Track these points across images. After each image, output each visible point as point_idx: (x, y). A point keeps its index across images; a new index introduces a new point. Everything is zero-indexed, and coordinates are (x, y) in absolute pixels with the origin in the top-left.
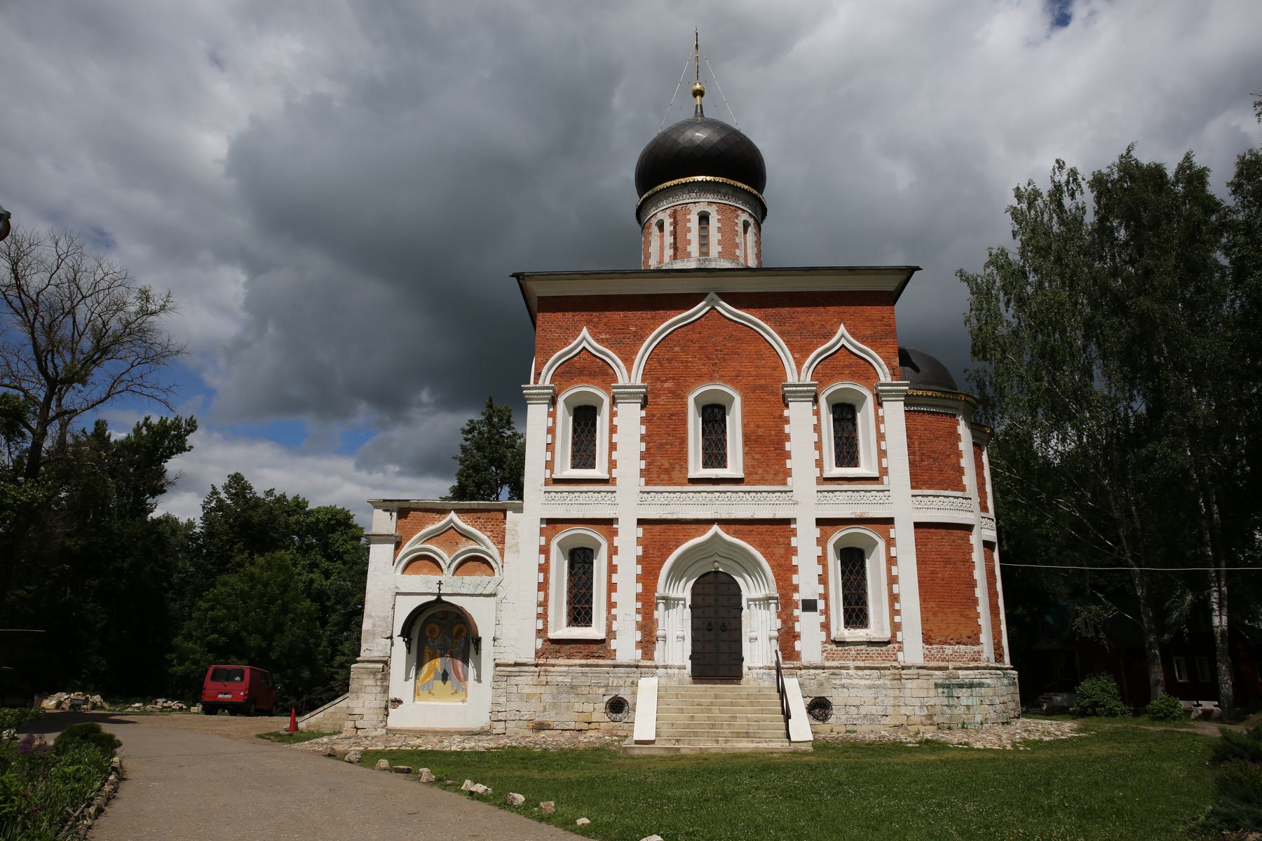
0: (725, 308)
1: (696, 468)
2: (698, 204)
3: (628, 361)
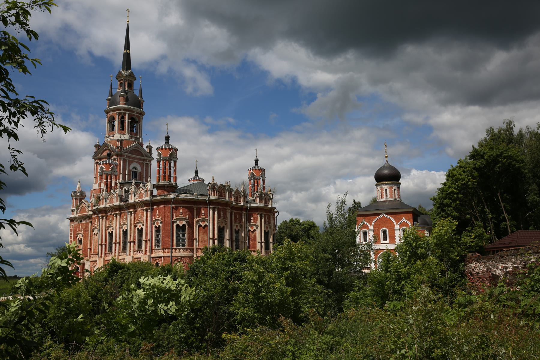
0: (385, 215)
1: (382, 241)
2: (386, 187)
3: (371, 225)
